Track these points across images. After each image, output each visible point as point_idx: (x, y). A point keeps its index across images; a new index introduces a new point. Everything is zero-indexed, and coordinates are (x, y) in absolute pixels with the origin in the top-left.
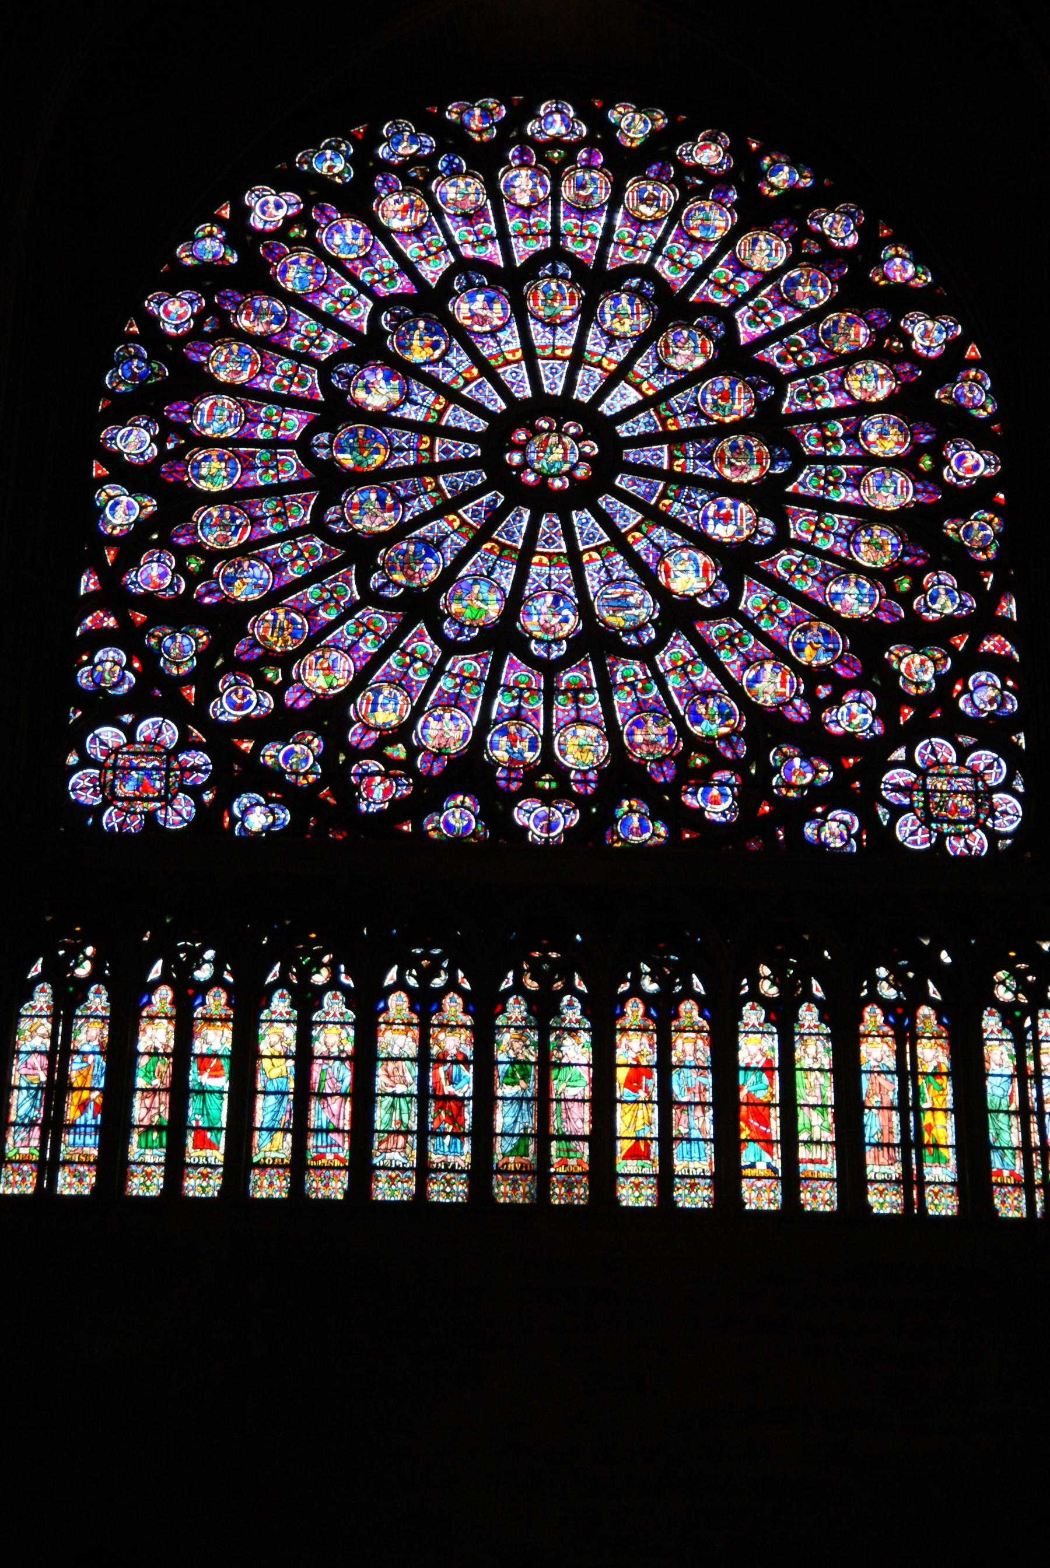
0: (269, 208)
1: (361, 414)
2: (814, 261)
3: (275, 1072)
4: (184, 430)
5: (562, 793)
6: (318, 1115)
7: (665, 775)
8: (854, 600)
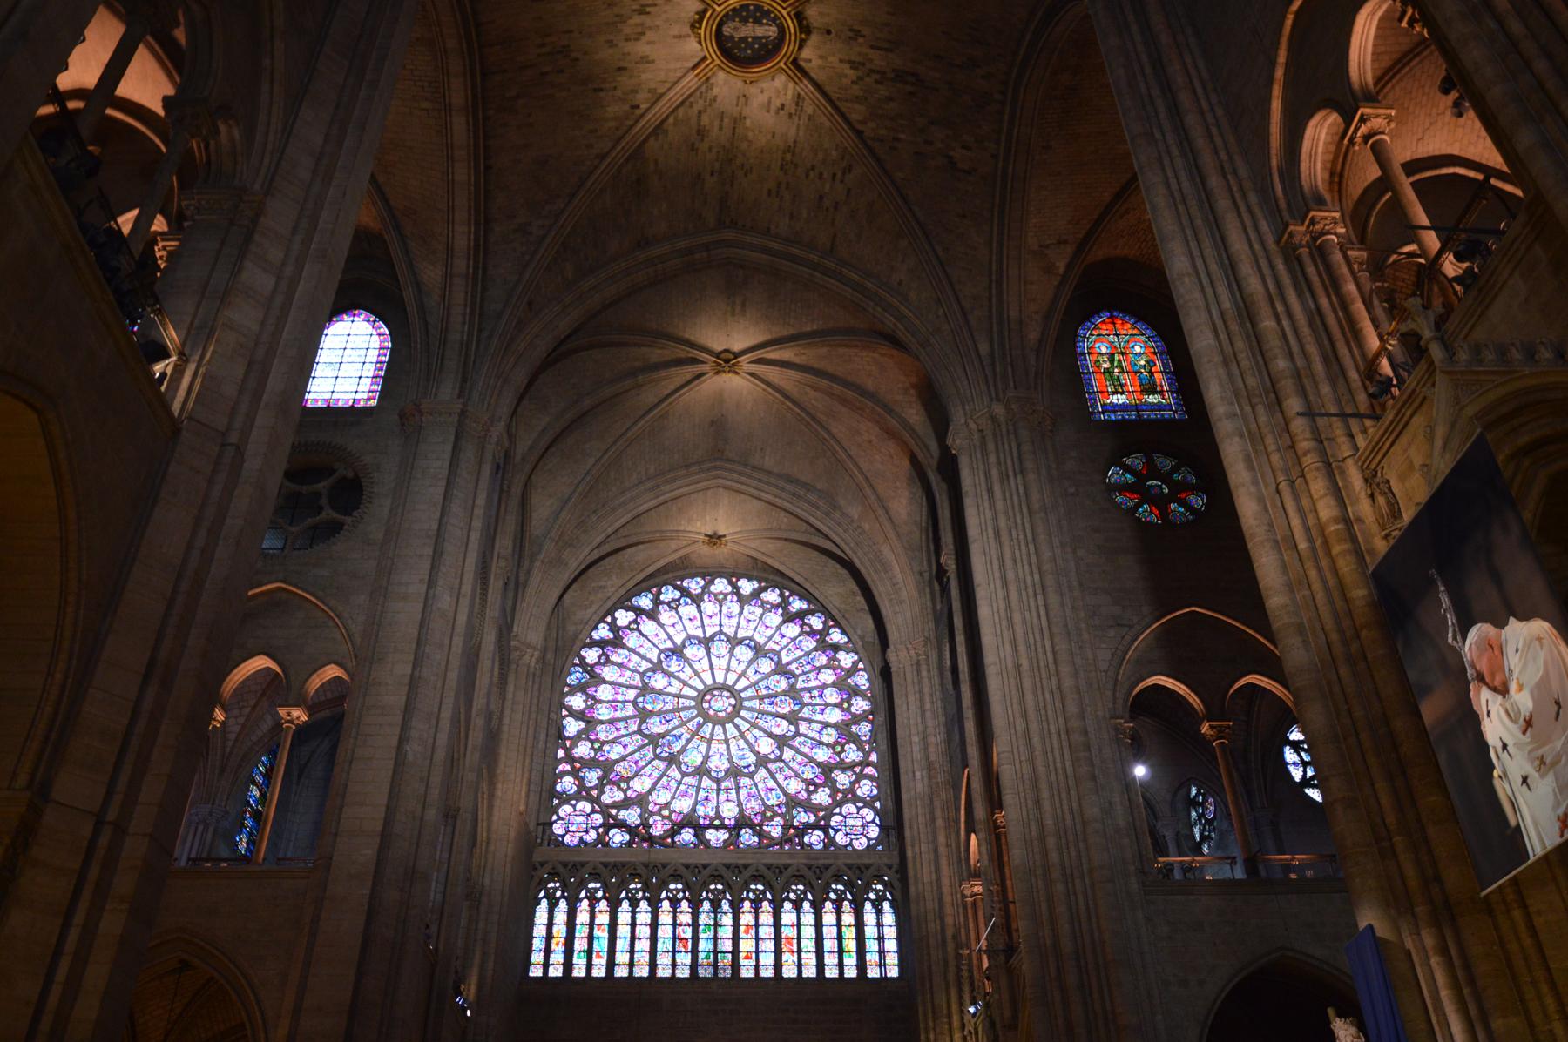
0: (624, 618)
1: (653, 690)
2: (808, 634)
3: (623, 931)
4: (593, 698)
5: (723, 826)
6: (638, 946)
7: (757, 820)
8: (822, 755)
